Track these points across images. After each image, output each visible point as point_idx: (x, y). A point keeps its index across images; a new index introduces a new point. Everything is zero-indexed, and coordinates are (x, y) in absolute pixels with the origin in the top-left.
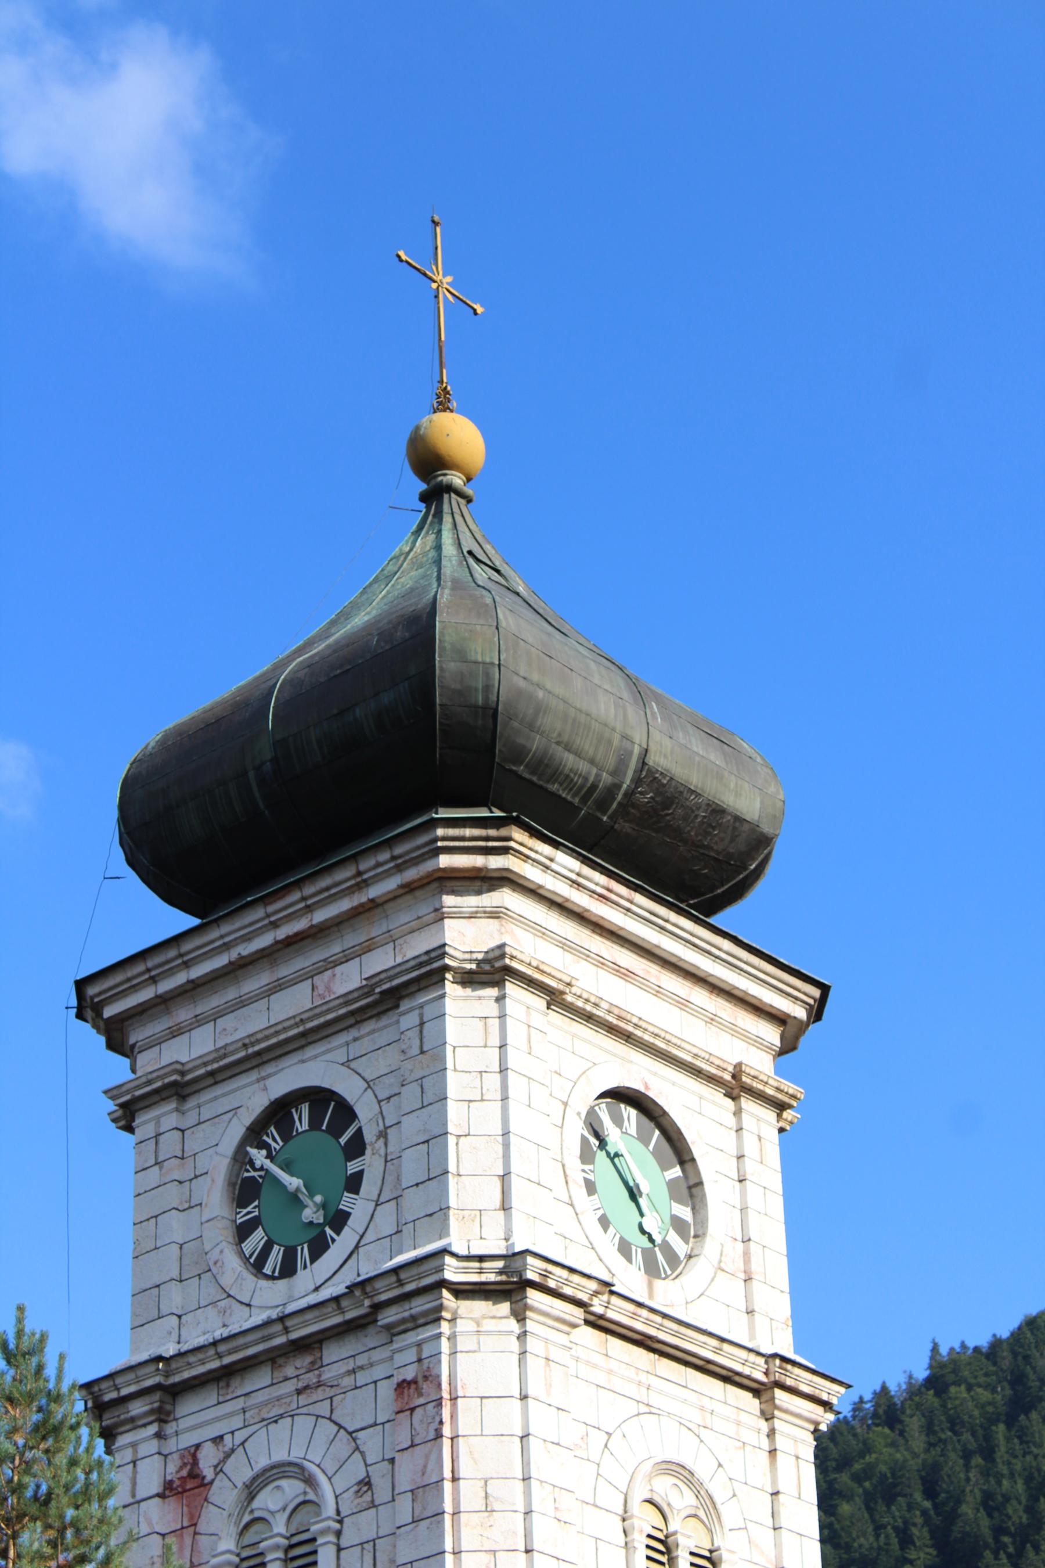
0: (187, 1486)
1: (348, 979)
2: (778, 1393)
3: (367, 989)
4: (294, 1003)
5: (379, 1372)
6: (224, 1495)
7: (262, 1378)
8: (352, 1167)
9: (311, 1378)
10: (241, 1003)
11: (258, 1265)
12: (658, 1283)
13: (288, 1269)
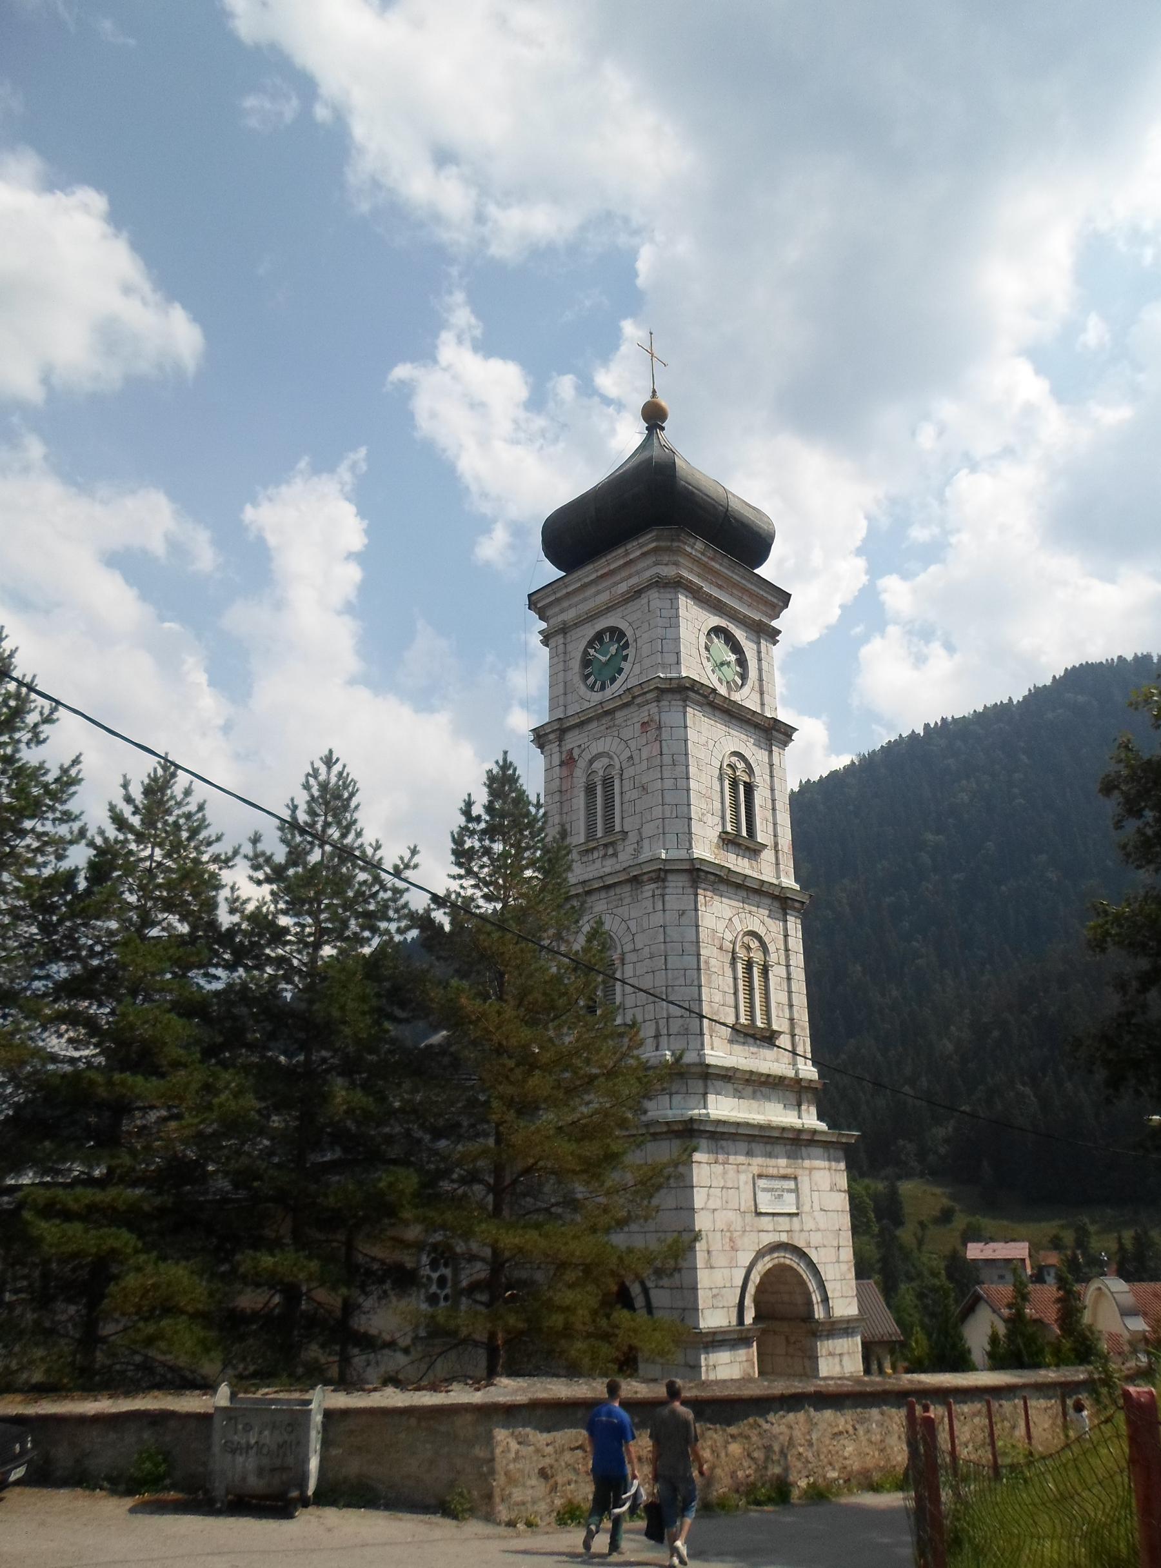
1: (623, 587)
2: (774, 733)
3: (628, 592)
4: (604, 597)
5: (635, 720)
6: (582, 764)
7: (594, 724)
8: (624, 653)
9: (611, 724)
10: (585, 600)
11: (592, 688)
12: (733, 693)
13: (603, 688)
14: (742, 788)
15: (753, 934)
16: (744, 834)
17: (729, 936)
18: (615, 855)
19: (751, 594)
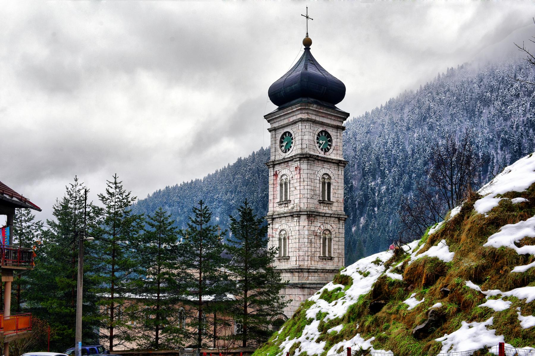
0: (276, 175)
4: (286, 122)
6: (279, 176)
13: (286, 152)
14: (326, 185)
15: (327, 230)
16: (326, 199)
17: (319, 231)
18: (288, 207)
19: (335, 116)
